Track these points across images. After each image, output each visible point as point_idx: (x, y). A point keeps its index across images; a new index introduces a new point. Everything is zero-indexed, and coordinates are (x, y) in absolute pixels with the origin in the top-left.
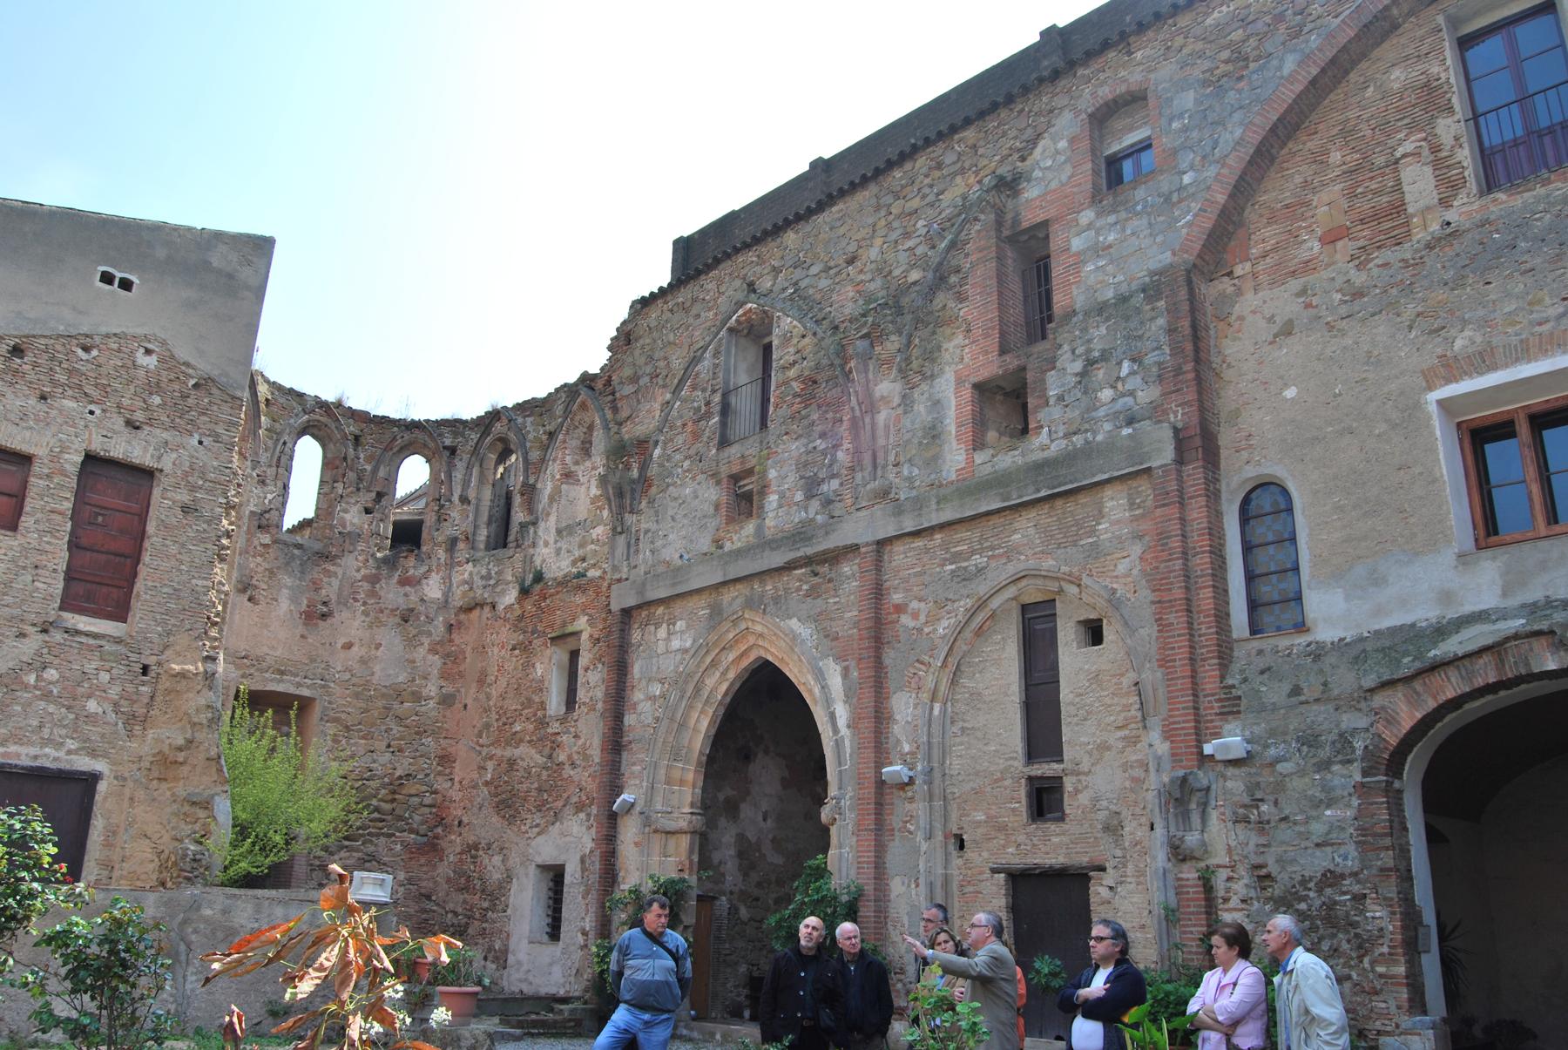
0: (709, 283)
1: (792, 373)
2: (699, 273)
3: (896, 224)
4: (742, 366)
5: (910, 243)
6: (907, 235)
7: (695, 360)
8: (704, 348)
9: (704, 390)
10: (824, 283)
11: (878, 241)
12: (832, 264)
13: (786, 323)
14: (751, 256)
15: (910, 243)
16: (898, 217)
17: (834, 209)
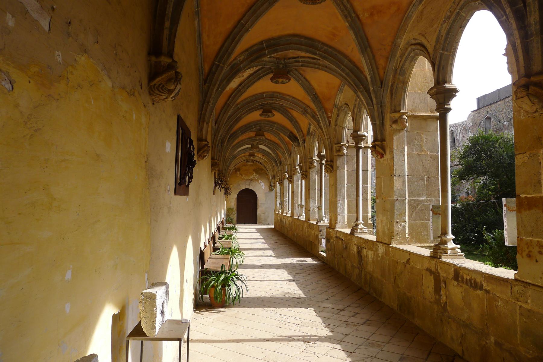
0: (482, 111)
1: (494, 127)
2: (480, 109)
3: (507, 107)
4: (488, 123)
5: (509, 111)
6: (508, 109)
7: (481, 123)
8: (482, 121)
9: (482, 127)
10: (498, 114)
11: (505, 109)
12: (499, 111)
13: (493, 119)
14: (487, 107)
15: (509, 111)
16: (507, 106)
17: (499, 103)
